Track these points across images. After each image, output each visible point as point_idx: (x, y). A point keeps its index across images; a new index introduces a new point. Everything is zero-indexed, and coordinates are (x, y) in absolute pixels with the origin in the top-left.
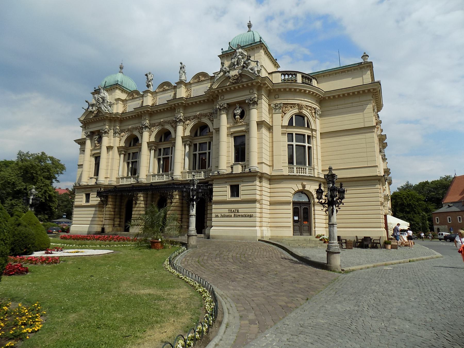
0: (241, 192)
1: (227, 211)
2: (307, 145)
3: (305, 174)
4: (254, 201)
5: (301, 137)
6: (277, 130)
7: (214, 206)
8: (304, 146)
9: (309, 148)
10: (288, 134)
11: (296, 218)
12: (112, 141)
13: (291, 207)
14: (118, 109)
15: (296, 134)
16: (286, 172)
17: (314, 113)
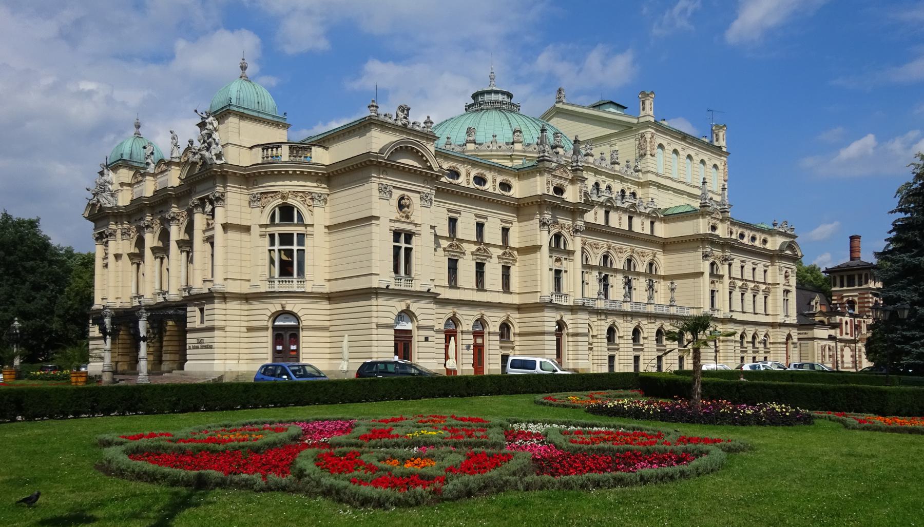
0: (206, 318)
1: (195, 341)
2: (295, 248)
3: (291, 290)
4: (212, 329)
5: (286, 239)
6: (256, 231)
7: (188, 336)
8: (292, 250)
9: (301, 252)
10: (270, 235)
11: (279, 348)
12: (120, 246)
13: (269, 333)
14: (124, 199)
15: (280, 234)
16: (264, 288)
17: (309, 201)
